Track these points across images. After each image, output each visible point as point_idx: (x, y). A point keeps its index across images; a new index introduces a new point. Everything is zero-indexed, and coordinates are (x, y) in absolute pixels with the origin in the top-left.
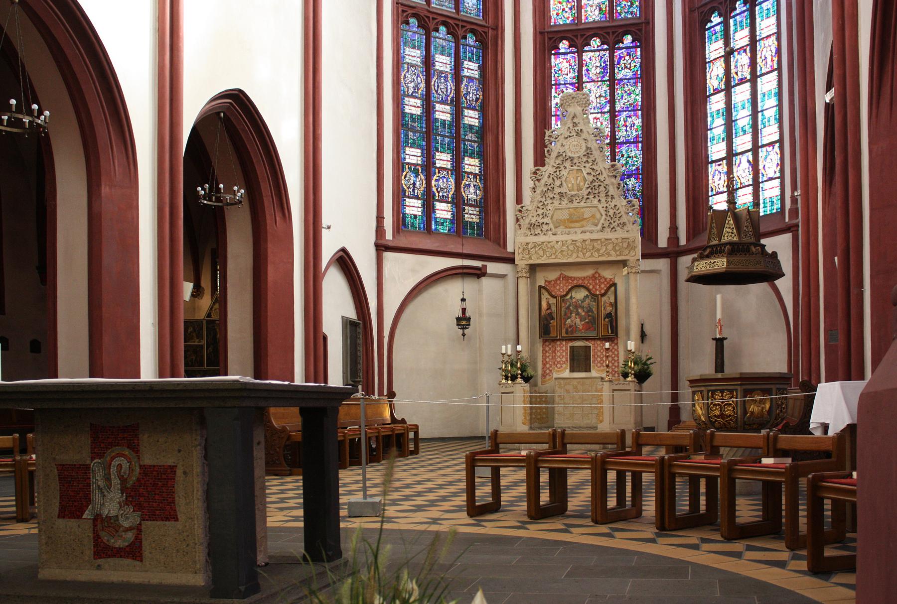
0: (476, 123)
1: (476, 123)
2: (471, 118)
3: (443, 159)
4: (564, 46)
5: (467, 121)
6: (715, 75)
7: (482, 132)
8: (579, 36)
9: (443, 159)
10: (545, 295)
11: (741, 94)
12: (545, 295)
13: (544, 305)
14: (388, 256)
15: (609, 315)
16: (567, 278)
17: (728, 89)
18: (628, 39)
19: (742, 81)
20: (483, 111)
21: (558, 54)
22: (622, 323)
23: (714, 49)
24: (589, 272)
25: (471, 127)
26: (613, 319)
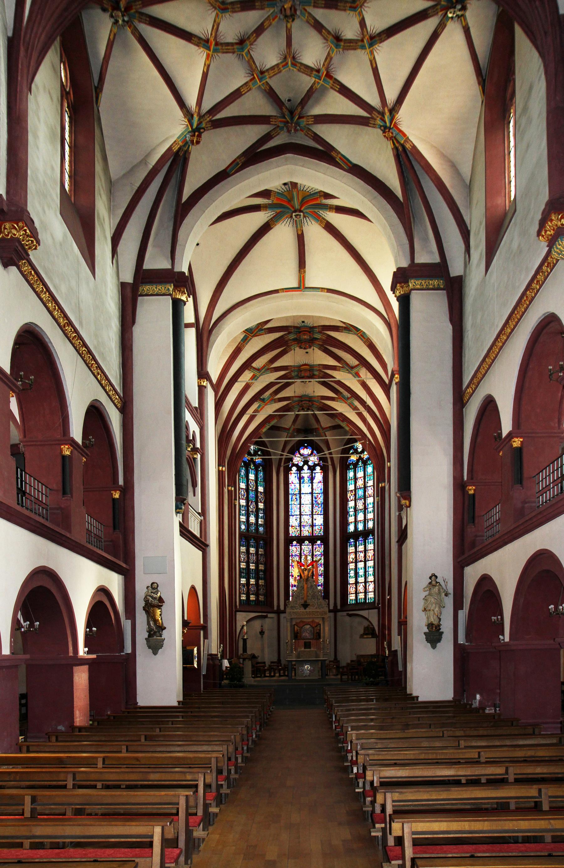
0: (263, 568)
1: (263, 568)
2: (261, 567)
3: (252, 581)
4: (295, 543)
5: (260, 568)
6: (351, 557)
7: (265, 571)
8: (301, 540)
9: (252, 581)
10: (296, 627)
11: (361, 565)
12: (296, 627)
13: (296, 629)
14: (238, 613)
15: (317, 633)
16: (303, 622)
17: (356, 562)
18: (319, 542)
19: (361, 561)
20: (265, 564)
21: (292, 546)
22: (322, 635)
23: (351, 549)
24: (311, 620)
25: (261, 570)
26: (319, 634)
